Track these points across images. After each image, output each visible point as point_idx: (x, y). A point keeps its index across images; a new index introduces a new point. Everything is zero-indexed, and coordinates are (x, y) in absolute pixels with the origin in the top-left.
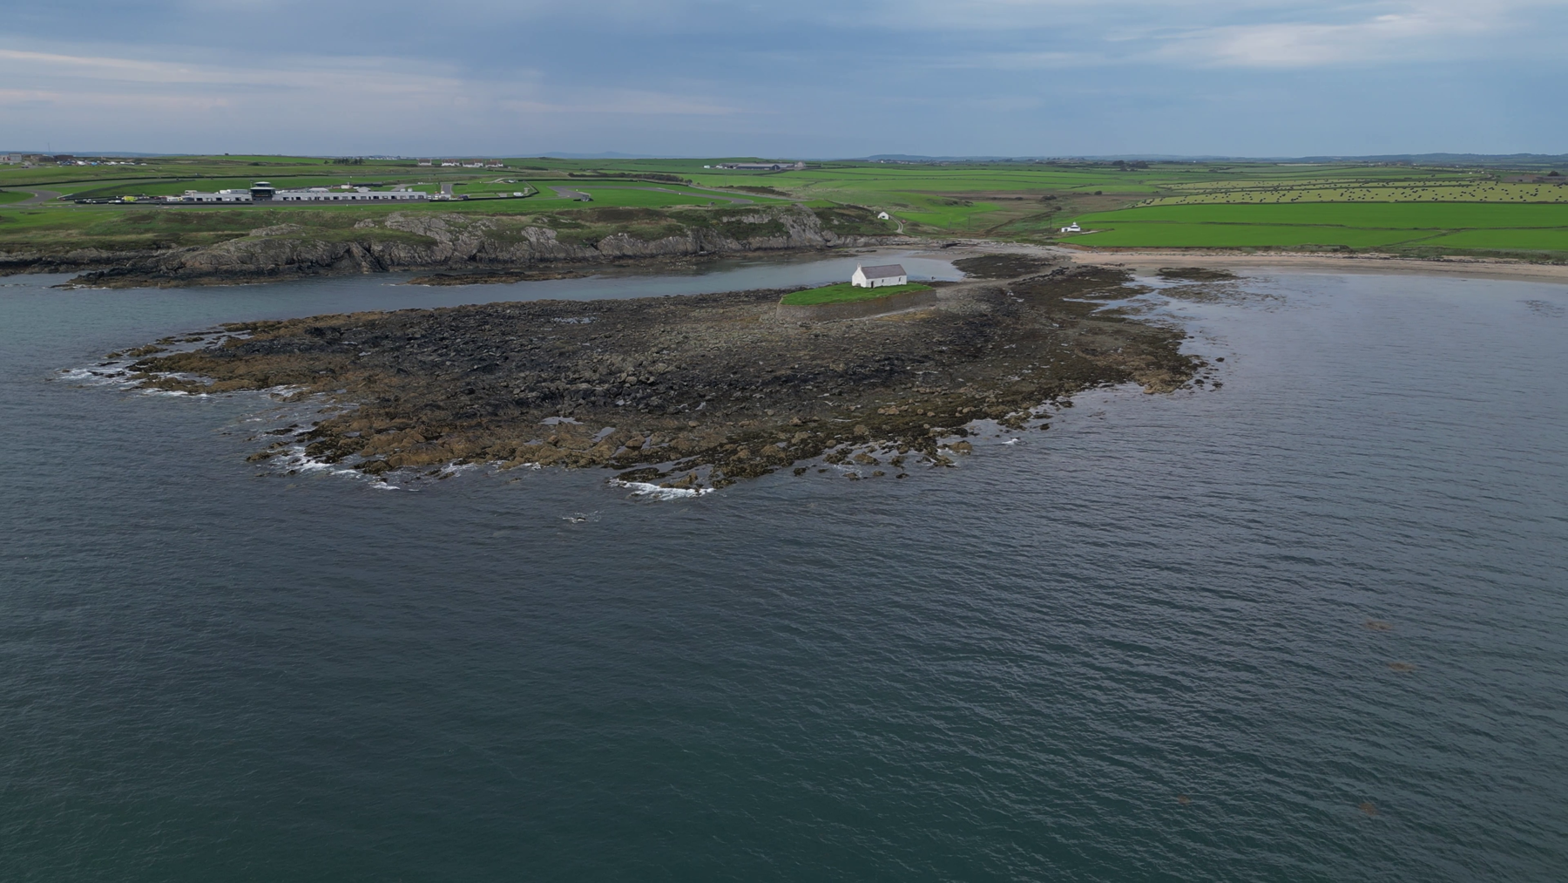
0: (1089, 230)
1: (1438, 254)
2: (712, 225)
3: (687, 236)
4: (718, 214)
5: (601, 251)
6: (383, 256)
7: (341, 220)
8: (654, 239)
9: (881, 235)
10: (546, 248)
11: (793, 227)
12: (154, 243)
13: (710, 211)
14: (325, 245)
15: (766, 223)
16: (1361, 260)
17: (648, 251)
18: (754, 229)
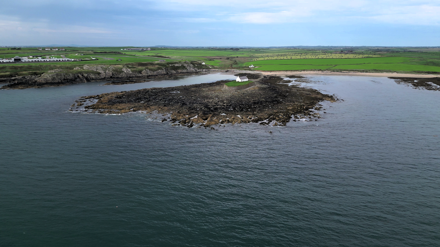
0: (256, 67)
1: (341, 71)
2: (168, 67)
3: (163, 70)
4: (168, 64)
5: (143, 74)
6: (88, 77)
7: (63, 67)
8: (155, 71)
9: (208, 69)
10: (129, 74)
11: (188, 67)
12: (11, 75)
13: (166, 63)
14: (72, 75)
16: (325, 72)
17: (154, 74)
18: (178, 68)
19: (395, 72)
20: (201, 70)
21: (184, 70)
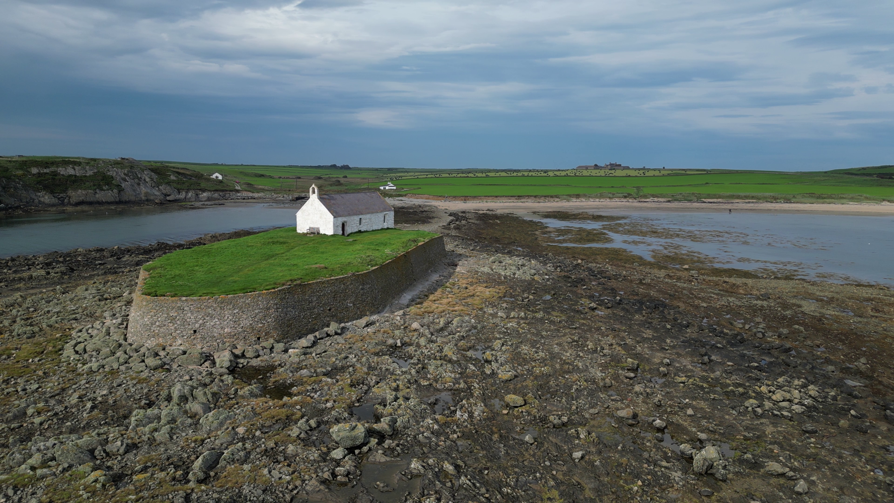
9: (223, 191)
15: (90, 176)
18: (74, 182)
19: (884, 200)
20: (190, 195)
21: (103, 193)
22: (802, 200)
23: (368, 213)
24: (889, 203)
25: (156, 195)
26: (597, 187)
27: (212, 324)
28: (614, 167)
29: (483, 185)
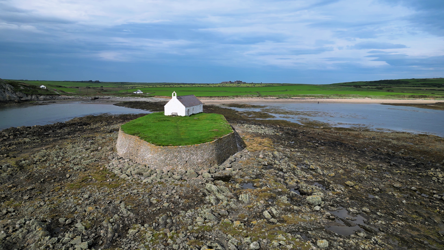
9: (51, 95)
19: (366, 97)
22: (334, 97)
23: (195, 105)
24: (368, 98)
25: (14, 98)
26: (239, 92)
27: (193, 158)
28: (239, 82)
29: (185, 91)
